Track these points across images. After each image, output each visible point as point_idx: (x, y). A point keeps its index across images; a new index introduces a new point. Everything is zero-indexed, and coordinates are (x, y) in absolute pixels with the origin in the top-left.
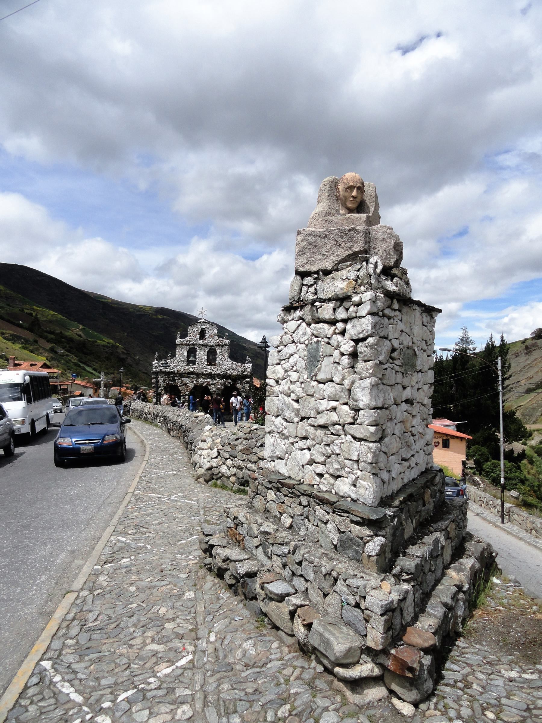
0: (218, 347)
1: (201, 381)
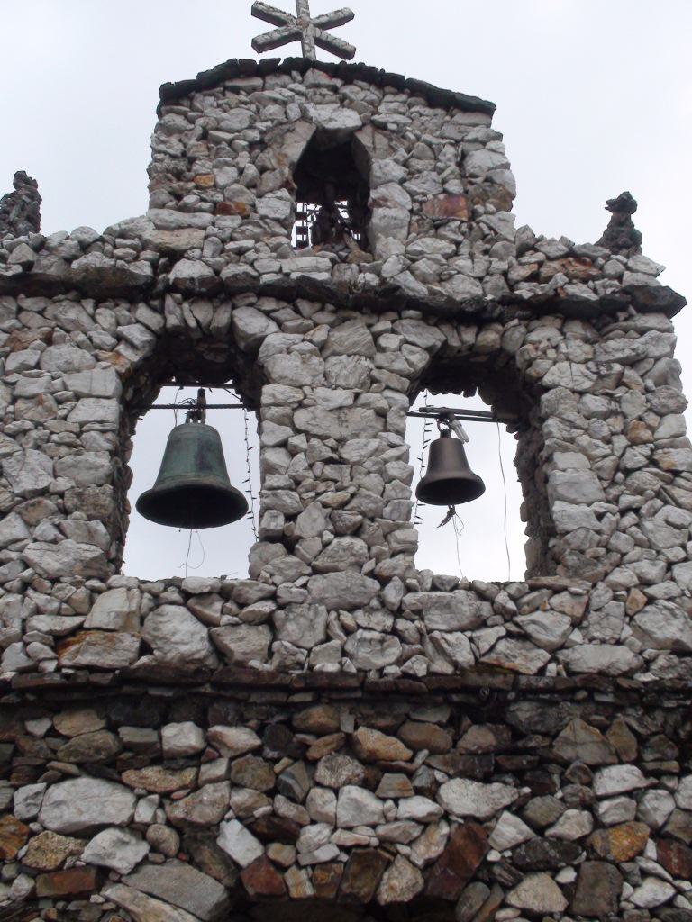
0: (545, 332)
1: (342, 811)
